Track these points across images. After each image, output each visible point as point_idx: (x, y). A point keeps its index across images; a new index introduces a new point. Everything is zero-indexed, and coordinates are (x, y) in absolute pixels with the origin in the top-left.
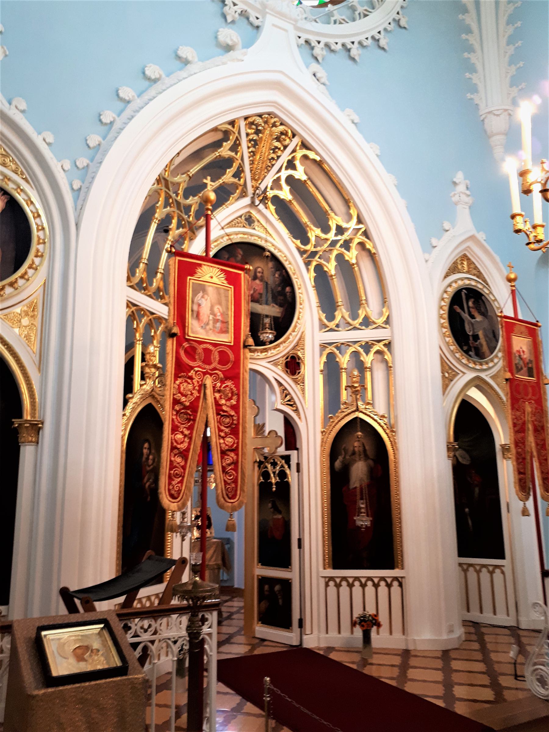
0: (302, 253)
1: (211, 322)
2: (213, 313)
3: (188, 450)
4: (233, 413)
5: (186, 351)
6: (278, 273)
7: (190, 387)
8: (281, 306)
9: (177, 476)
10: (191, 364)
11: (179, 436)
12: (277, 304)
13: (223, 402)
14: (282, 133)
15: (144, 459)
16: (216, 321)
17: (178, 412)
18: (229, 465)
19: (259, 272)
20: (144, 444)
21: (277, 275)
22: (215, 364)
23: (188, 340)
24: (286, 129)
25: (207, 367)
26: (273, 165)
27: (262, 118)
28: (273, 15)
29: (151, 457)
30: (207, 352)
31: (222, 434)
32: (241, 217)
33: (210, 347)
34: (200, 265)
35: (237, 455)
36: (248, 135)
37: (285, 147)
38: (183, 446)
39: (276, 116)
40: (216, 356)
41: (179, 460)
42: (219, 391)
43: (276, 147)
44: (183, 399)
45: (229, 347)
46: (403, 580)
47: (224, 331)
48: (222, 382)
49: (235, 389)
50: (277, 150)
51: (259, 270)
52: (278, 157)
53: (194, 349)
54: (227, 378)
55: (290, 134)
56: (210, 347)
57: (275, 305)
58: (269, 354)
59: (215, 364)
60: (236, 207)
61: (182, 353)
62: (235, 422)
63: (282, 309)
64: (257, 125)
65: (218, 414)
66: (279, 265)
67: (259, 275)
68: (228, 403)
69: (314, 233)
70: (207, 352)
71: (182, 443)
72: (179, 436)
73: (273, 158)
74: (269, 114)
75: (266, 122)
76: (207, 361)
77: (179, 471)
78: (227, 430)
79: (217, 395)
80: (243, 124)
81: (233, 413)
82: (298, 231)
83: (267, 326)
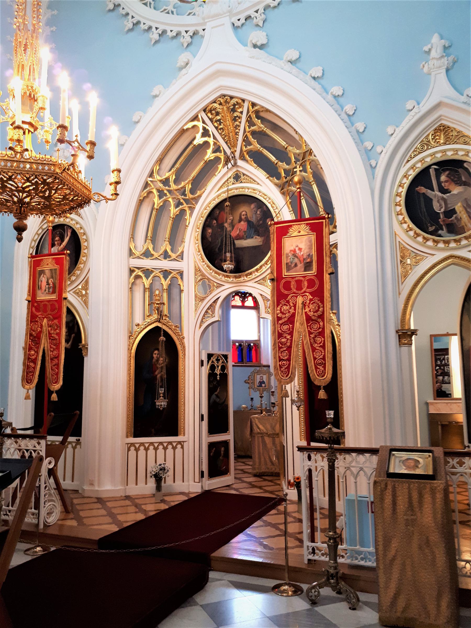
0: (192, 209)
1: (47, 289)
2: (48, 284)
3: (36, 359)
4: (57, 337)
5: (36, 307)
6: (260, 210)
7: (36, 326)
8: (261, 236)
9: (30, 372)
10: (37, 314)
11: (33, 352)
12: (259, 236)
13: (52, 332)
14: (234, 105)
15: (154, 360)
16: (49, 288)
17: (32, 340)
18: (54, 366)
19: (244, 215)
20: (153, 352)
21: (258, 213)
22: (49, 312)
23: (37, 302)
24: (237, 100)
25: (45, 314)
26: (239, 130)
27: (216, 103)
28: (209, 21)
29: (161, 359)
30: (45, 306)
31: (52, 349)
32: (230, 178)
33: (47, 303)
34: (42, 259)
35: (58, 360)
36: (211, 120)
37: (241, 113)
38: (33, 357)
39: (225, 96)
40: (49, 307)
41: (32, 364)
42: (50, 326)
43: (235, 117)
44: (34, 333)
45: (56, 301)
46: (185, 443)
47: (54, 292)
48: (52, 321)
49: (58, 324)
50: (237, 118)
51: (244, 213)
52: (240, 122)
53: (39, 305)
54: (55, 318)
55: (240, 101)
56: (47, 303)
57: (257, 237)
58: (253, 276)
59: (49, 312)
60: (223, 172)
61: (34, 309)
62: (58, 342)
63: (263, 238)
64: (215, 109)
65: (50, 339)
66: (260, 204)
67: (243, 217)
68: (55, 333)
69: (283, 166)
70: (45, 306)
71: (33, 355)
72: (33, 352)
73: (237, 125)
74: (220, 97)
75: (220, 104)
76: (45, 311)
77: (31, 369)
78: (54, 347)
79: (50, 329)
80: (203, 114)
81: (57, 337)
82: (272, 171)
83: (228, 259)
